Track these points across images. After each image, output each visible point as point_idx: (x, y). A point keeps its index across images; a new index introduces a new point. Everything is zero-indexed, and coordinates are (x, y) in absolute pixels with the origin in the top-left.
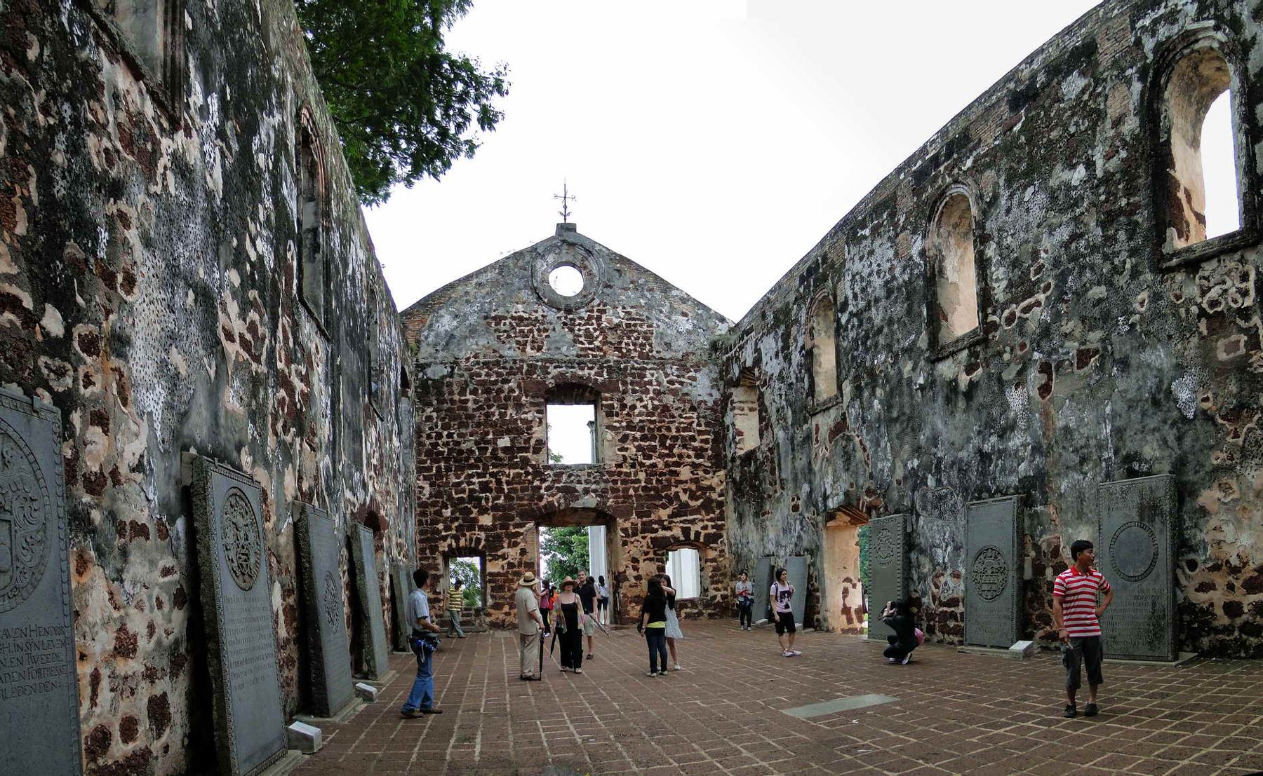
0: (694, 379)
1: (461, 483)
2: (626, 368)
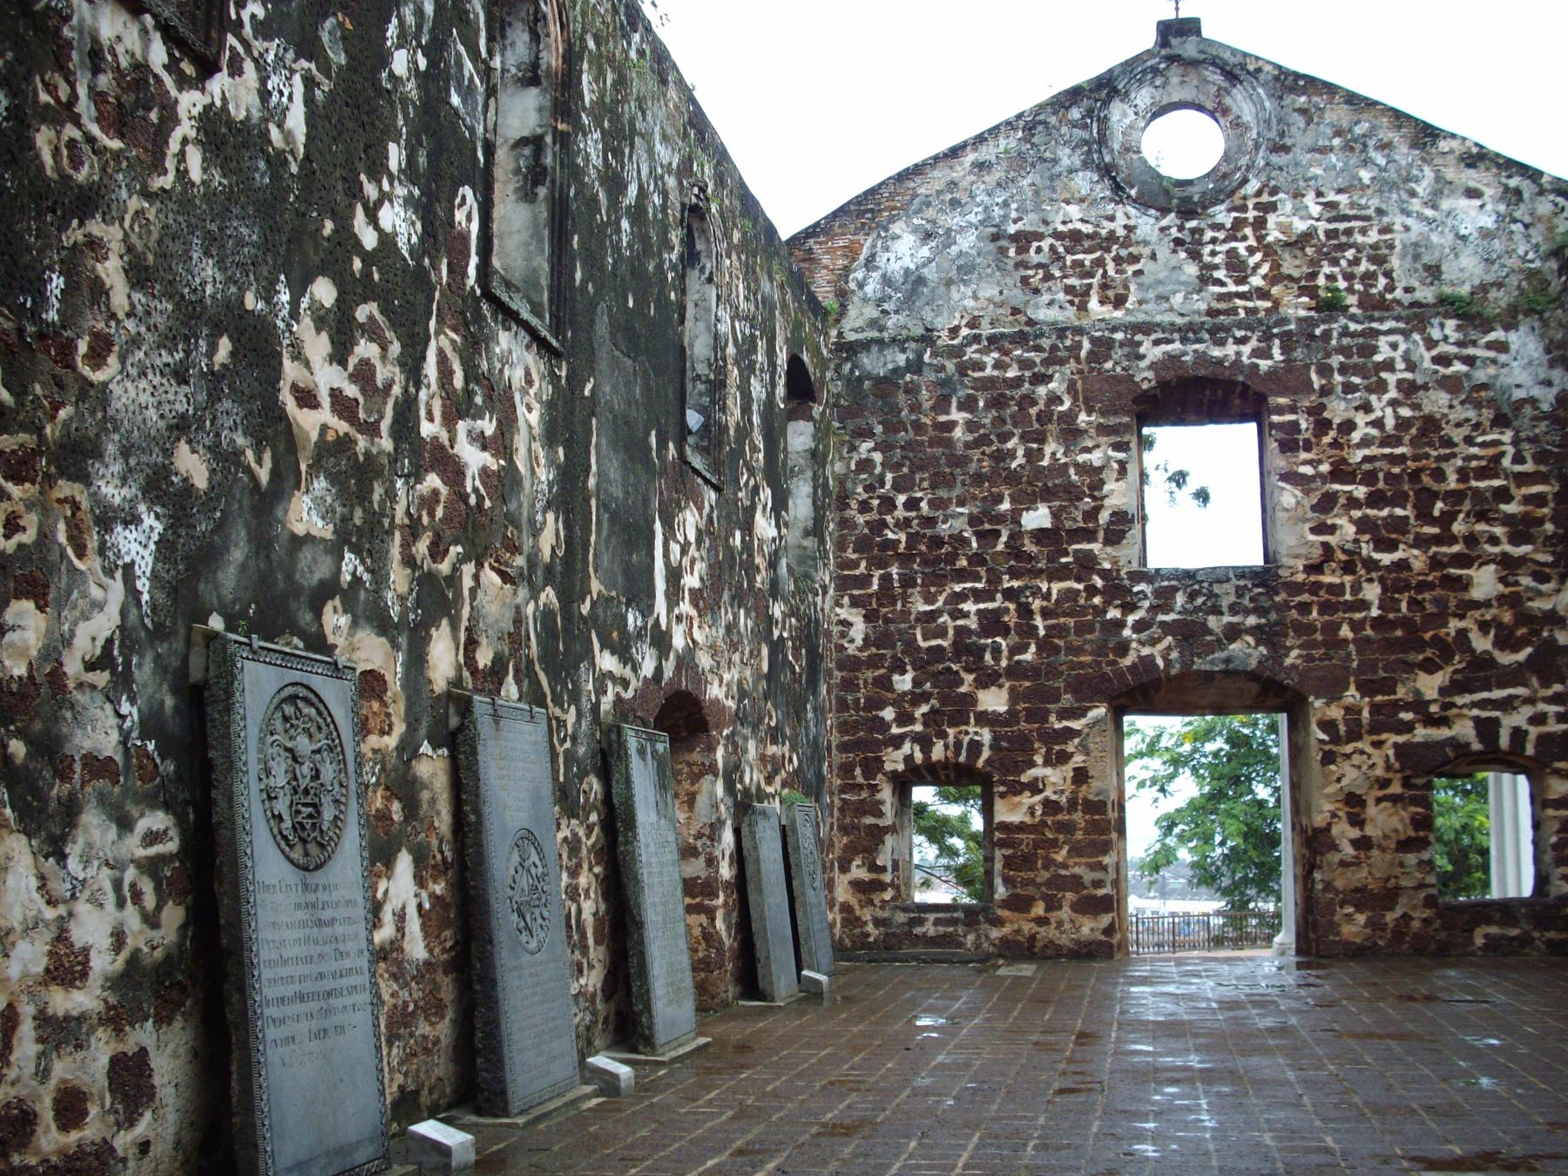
1: (939, 612)
2: (1327, 335)
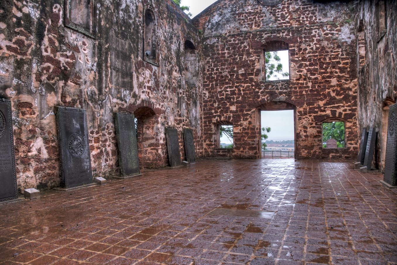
0: (340, 31)
2: (302, 30)
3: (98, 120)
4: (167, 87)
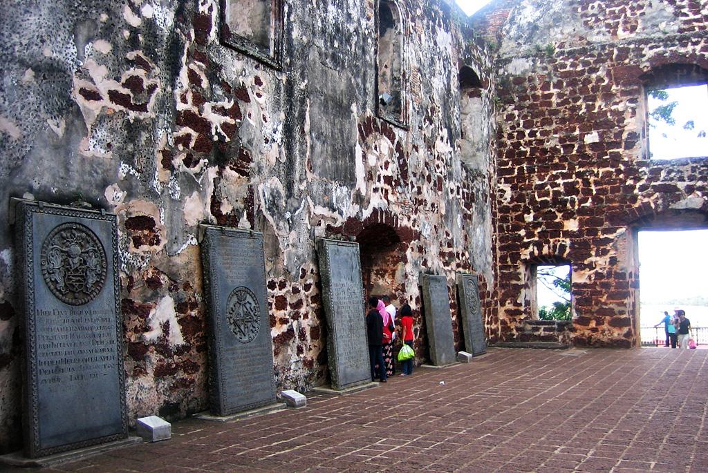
1: (545, 185)
3: (285, 255)
4: (423, 176)
